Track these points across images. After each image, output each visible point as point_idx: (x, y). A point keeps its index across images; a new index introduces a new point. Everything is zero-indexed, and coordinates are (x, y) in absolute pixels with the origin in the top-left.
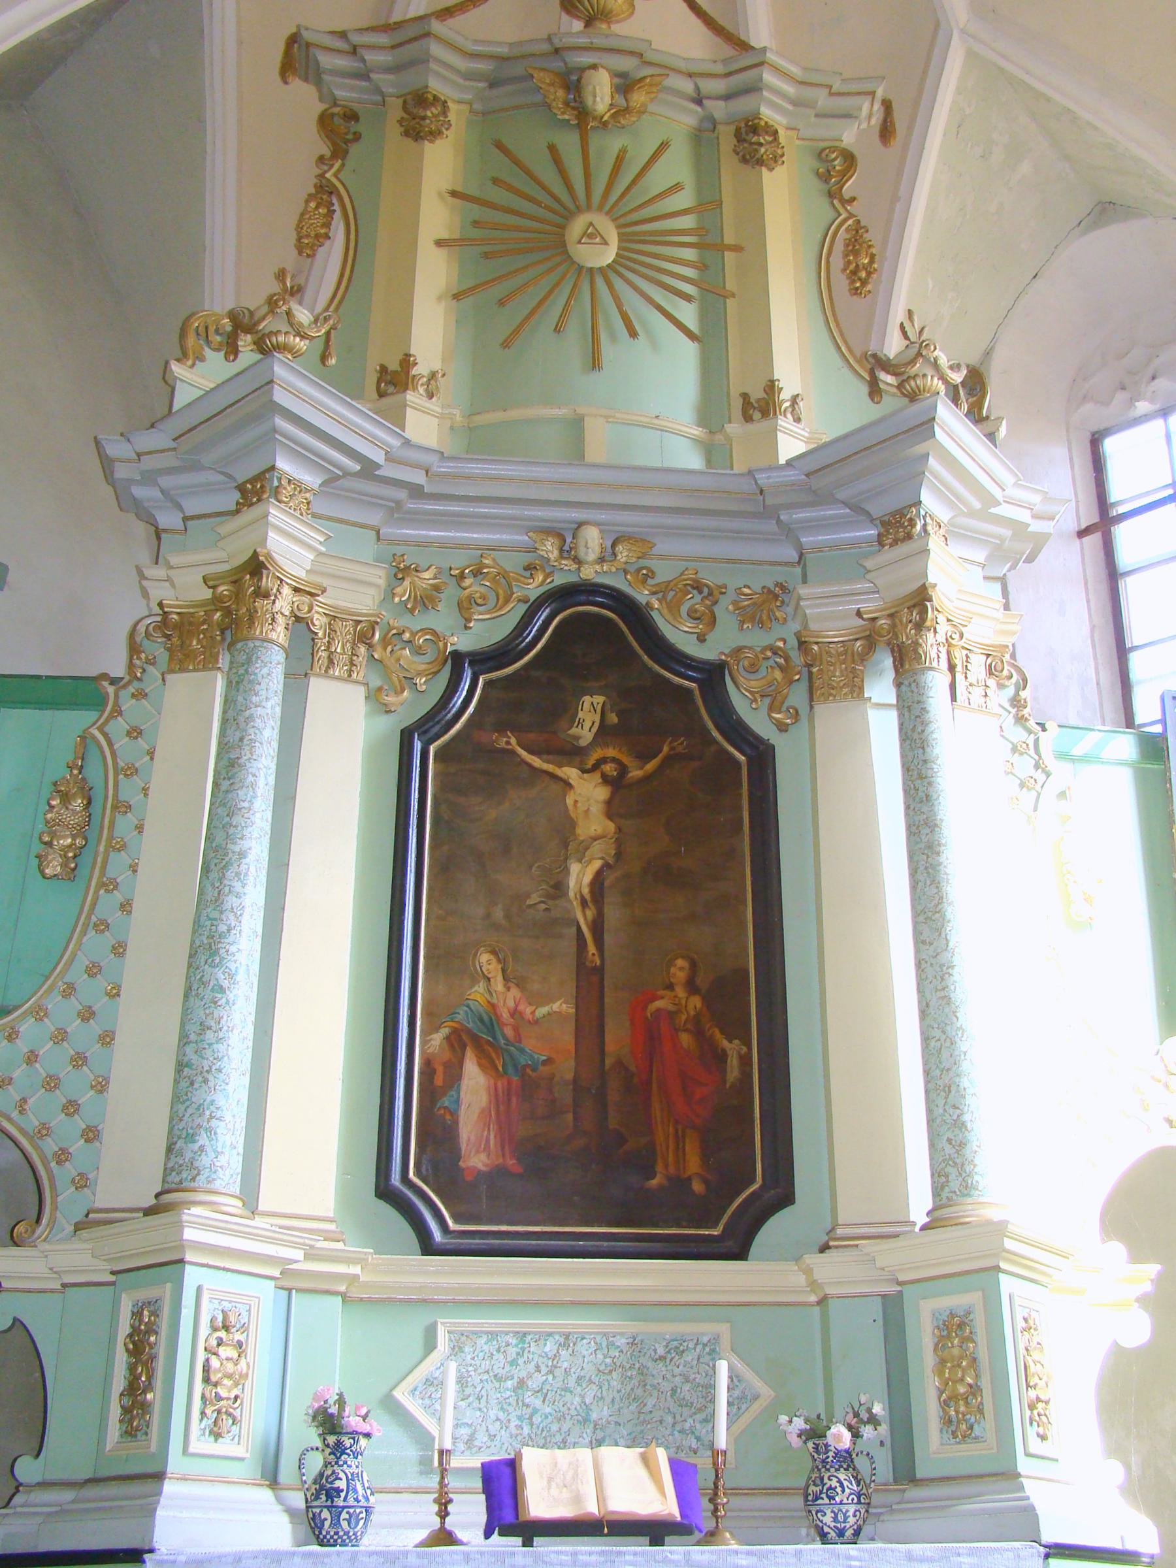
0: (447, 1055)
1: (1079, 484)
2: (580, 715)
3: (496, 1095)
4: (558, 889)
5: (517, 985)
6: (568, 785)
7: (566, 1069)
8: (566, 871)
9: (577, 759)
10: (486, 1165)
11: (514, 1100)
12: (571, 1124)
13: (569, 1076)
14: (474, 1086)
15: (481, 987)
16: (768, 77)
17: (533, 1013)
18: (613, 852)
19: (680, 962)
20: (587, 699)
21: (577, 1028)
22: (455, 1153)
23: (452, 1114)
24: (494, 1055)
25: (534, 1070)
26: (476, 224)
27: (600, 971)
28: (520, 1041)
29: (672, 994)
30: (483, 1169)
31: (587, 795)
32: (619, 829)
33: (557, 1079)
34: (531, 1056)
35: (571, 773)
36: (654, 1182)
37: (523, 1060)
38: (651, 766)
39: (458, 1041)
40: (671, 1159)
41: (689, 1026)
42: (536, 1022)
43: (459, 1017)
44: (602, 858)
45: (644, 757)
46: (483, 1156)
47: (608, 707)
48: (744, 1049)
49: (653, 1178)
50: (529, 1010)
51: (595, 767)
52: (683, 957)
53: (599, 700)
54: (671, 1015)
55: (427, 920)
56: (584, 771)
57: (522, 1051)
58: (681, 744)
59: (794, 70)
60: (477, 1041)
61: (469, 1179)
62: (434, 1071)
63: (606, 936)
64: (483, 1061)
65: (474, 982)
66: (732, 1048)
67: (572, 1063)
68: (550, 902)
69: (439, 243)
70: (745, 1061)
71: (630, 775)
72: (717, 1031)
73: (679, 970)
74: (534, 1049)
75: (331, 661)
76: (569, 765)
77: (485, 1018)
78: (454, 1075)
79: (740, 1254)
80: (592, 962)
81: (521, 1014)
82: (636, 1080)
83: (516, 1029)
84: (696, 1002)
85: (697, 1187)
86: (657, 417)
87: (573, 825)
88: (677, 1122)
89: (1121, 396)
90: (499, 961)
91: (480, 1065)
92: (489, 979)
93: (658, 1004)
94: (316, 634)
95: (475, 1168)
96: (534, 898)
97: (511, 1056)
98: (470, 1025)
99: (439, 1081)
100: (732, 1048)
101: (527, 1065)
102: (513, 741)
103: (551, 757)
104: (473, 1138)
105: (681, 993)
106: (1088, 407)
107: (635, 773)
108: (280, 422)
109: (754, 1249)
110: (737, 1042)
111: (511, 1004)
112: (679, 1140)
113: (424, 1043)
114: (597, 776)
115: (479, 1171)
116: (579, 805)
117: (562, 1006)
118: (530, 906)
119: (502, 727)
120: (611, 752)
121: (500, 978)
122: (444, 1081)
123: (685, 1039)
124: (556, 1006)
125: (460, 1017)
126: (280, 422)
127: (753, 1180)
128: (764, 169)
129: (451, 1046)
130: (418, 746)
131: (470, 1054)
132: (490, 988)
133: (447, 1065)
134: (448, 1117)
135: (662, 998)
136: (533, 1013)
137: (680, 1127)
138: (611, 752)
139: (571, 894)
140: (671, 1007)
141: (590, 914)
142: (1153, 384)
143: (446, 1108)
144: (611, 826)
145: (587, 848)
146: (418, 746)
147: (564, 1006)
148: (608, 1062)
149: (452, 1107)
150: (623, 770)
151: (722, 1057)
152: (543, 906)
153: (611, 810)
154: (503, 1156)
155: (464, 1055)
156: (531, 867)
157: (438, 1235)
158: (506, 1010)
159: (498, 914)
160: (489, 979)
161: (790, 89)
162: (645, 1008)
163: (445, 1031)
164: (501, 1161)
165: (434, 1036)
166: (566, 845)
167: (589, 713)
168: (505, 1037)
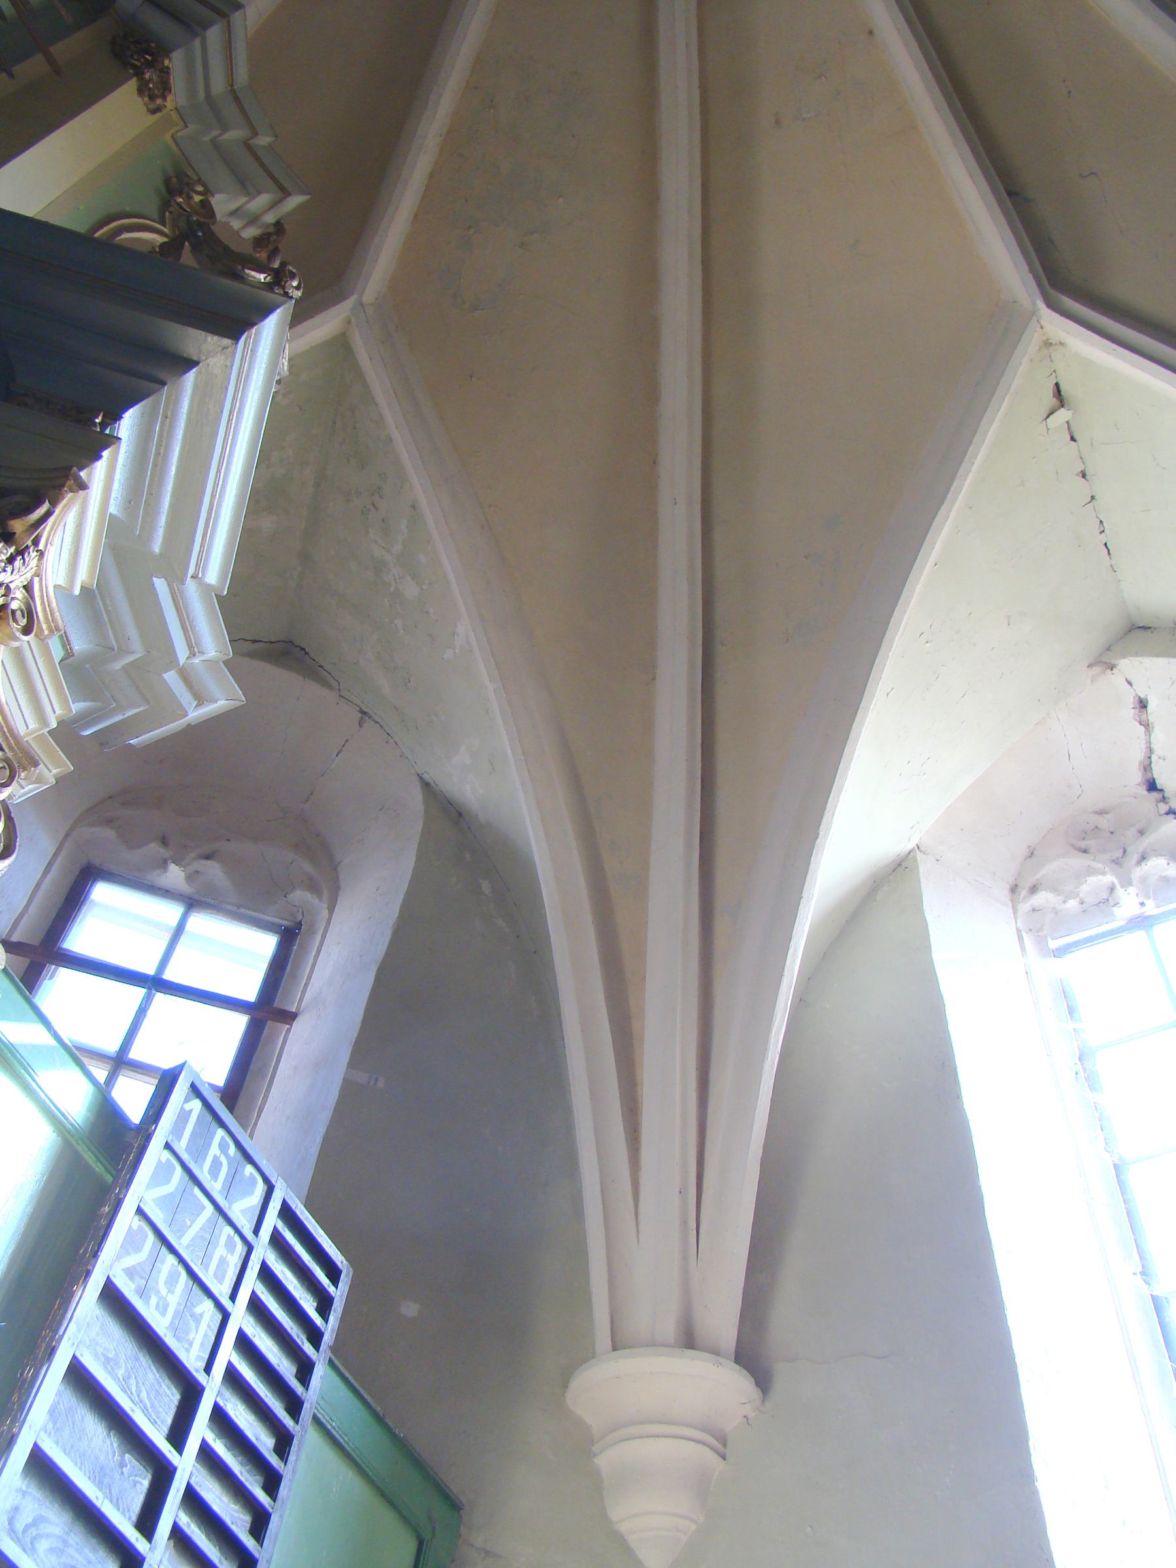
1: (40, 894)
16: (214, 34)
59: (242, 75)
89: (154, 848)
106: (109, 833)
128: (132, 85)
142: (204, 862)
161: (218, 85)
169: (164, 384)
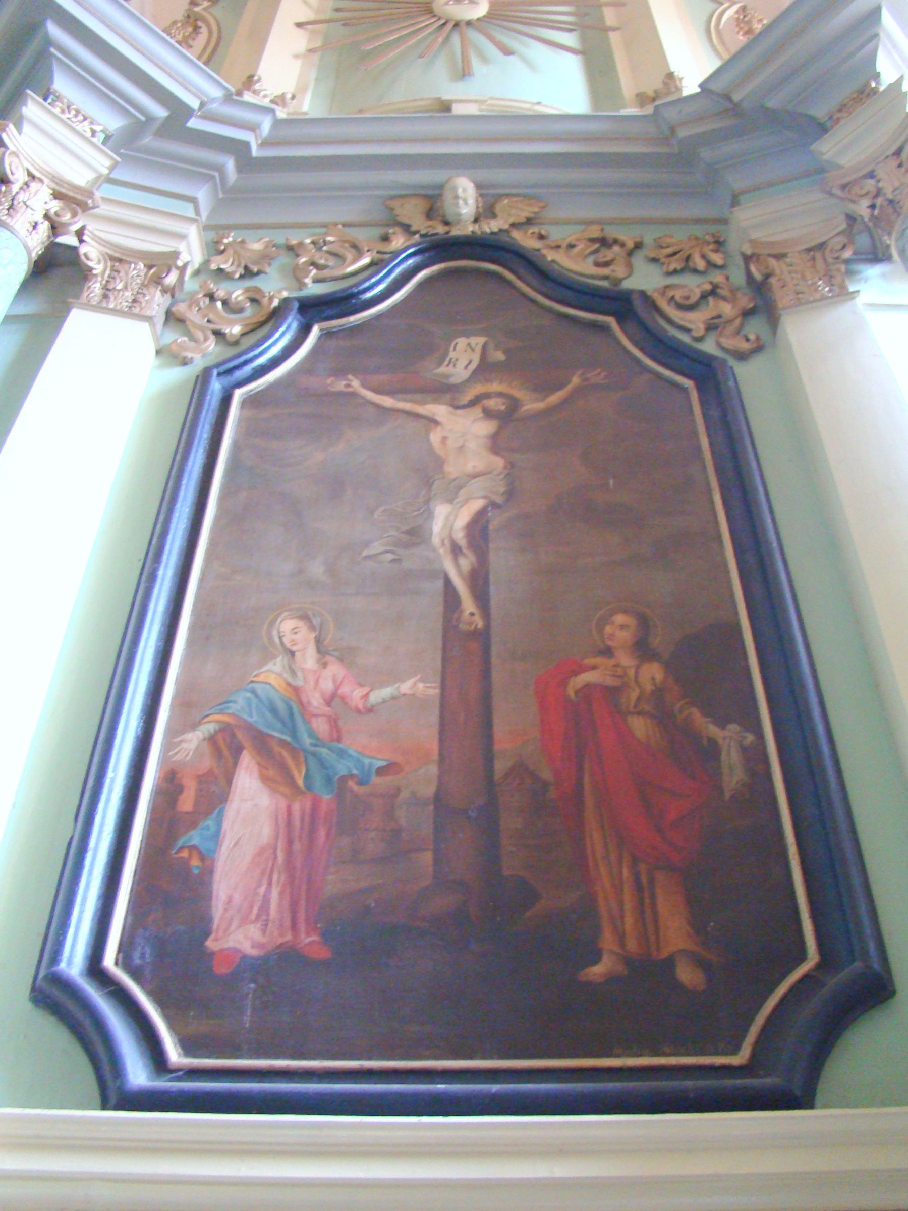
0: (207, 763)
2: (452, 355)
3: (289, 822)
4: (415, 535)
5: (341, 660)
6: (433, 422)
7: (424, 779)
8: (430, 515)
9: (448, 396)
10: (260, 946)
11: (322, 833)
12: (431, 869)
13: (429, 790)
14: (251, 811)
15: (278, 665)
17: (366, 696)
18: (502, 490)
19: (620, 619)
20: (462, 342)
21: (442, 717)
22: (202, 926)
23: (202, 857)
24: (290, 762)
25: (361, 783)
26: (337, 10)
27: (483, 637)
28: (339, 740)
29: (612, 662)
30: (248, 949)
31: (463, 437)
32: (511, 465)
33: (405, 794)
34: (358, 761)
35: (439, 410)
36: (597, 971)
37: (342, 768)
38: (555, 398)
39: (227, 746)
40: (629, 921)
41: (647, 708)
42: (370, 710)
43: (234, 708)
44: (485, 497)
45: (544, 388)
46: (254, 931)
47: (491, 346)
48: (750, 738)
49: (596, 957)
50: (358, 693)
51: (473, 403)
52: (625, 612)
53: (478, 341)
54: (611, 693)
55: (202, 580)
56: (457, 407)
57: (342, 754)
58: (597, 376)
60: (262, 744)
61: (222, 970)
62: (180, 789)
63: (492, 589)
64: (271, 773)
65: (268, 656)
66: (729, 739)
67: (434, 769)
68: (401, 551)
69: (299, 25)
70: (755, 757)
71: (525, 408)
72: (696, 713)
73: (621, 629)
74: (363, 749)
75: (105, 296)
76: (436, 401)
77: (281, 707)
78: (214, 794)
79: (796, 1097)
80: (471, 623)
81: (343, 699)
82: (552, 793)
83: (334, 722)
84: (653, 672)
85: (687, 975)
86: (539, 103)
87: (440, 463)
88: (635, 860)
90: (312, 628)
91: (265, 779)
92: (292, 654)
93: (588, 677)
94: (91, 269)
95: (236, 951)
96: (376, 547)
97: (322, 763)
98: (254, 719)
99: (186, 803)
100: (729, 739)
101: (352, 776)
102: (356, 384)
103: (409, 396)
104: (237, 898)
105: (626, 660)
107: (532, 404)
108: (53, 30)
109: (823, 1089)
110: (734, 727)
111: (327, 685)
112: (643, 893)
113: (168, 746)
114: (477, 412)
115: (245, 956)
116: (449, 442)
117: (419, 686)
118: (367, 557)
119: (340, 372)
120: (495, 387)
121: (311, 651)
122: (197, 803)
123: (639, 727)
124: (406, 687)
125: (239, 705)
126: (53, 30)
127: (802, 957)
129: (217, 752)
130: (216, 386)
131: (247, 760)
132: (294, 663)
133: (204, 779)
134: (195, 862)
135: (594, 668)
136: (366, 696)
137: (642, 867)
138: (495, 387)
139: (436, 540)
140: (610, 681)
141: (467, 562)
143: (194, 847)
144: (499, 462)
145: (460, 488)
146: (216, 386)
147: (421, 686)
148: (501, 766)
149: (203, 847)
150: (514, 404)
151: (713, 751)
152: (390, 556)
153: (495, 445)
154: (294, 927)
155: (236, 764)
156: (372, 512)
157: (138, 1074)
158: (317, 695)
159: (316, 569)
160: (292, 654)
162: (564, 683)
163: (209, 728)
164: (289, 937)
165: (189, 736)
166: (428, 483)
167: (463, 356)
168: (311, 734)
169: (876, 35)
